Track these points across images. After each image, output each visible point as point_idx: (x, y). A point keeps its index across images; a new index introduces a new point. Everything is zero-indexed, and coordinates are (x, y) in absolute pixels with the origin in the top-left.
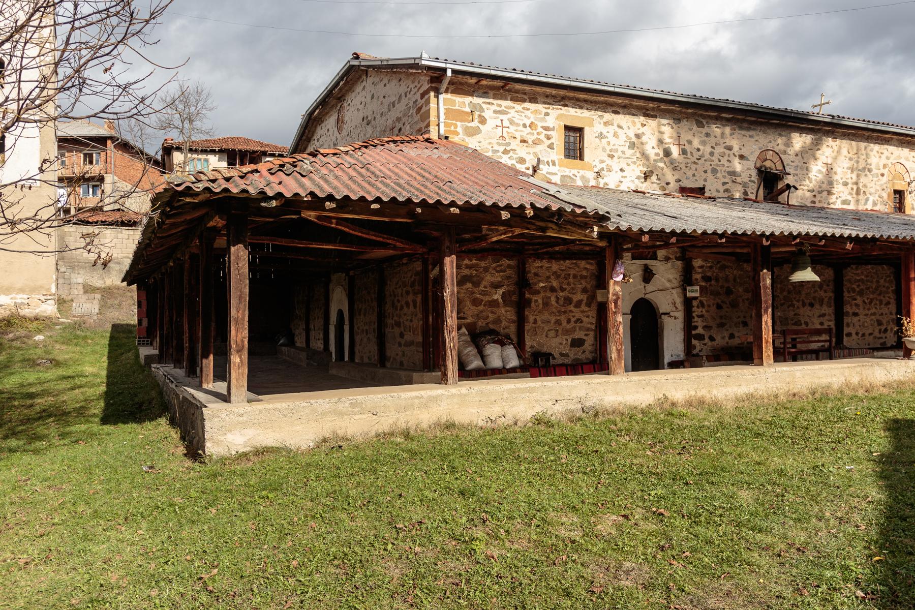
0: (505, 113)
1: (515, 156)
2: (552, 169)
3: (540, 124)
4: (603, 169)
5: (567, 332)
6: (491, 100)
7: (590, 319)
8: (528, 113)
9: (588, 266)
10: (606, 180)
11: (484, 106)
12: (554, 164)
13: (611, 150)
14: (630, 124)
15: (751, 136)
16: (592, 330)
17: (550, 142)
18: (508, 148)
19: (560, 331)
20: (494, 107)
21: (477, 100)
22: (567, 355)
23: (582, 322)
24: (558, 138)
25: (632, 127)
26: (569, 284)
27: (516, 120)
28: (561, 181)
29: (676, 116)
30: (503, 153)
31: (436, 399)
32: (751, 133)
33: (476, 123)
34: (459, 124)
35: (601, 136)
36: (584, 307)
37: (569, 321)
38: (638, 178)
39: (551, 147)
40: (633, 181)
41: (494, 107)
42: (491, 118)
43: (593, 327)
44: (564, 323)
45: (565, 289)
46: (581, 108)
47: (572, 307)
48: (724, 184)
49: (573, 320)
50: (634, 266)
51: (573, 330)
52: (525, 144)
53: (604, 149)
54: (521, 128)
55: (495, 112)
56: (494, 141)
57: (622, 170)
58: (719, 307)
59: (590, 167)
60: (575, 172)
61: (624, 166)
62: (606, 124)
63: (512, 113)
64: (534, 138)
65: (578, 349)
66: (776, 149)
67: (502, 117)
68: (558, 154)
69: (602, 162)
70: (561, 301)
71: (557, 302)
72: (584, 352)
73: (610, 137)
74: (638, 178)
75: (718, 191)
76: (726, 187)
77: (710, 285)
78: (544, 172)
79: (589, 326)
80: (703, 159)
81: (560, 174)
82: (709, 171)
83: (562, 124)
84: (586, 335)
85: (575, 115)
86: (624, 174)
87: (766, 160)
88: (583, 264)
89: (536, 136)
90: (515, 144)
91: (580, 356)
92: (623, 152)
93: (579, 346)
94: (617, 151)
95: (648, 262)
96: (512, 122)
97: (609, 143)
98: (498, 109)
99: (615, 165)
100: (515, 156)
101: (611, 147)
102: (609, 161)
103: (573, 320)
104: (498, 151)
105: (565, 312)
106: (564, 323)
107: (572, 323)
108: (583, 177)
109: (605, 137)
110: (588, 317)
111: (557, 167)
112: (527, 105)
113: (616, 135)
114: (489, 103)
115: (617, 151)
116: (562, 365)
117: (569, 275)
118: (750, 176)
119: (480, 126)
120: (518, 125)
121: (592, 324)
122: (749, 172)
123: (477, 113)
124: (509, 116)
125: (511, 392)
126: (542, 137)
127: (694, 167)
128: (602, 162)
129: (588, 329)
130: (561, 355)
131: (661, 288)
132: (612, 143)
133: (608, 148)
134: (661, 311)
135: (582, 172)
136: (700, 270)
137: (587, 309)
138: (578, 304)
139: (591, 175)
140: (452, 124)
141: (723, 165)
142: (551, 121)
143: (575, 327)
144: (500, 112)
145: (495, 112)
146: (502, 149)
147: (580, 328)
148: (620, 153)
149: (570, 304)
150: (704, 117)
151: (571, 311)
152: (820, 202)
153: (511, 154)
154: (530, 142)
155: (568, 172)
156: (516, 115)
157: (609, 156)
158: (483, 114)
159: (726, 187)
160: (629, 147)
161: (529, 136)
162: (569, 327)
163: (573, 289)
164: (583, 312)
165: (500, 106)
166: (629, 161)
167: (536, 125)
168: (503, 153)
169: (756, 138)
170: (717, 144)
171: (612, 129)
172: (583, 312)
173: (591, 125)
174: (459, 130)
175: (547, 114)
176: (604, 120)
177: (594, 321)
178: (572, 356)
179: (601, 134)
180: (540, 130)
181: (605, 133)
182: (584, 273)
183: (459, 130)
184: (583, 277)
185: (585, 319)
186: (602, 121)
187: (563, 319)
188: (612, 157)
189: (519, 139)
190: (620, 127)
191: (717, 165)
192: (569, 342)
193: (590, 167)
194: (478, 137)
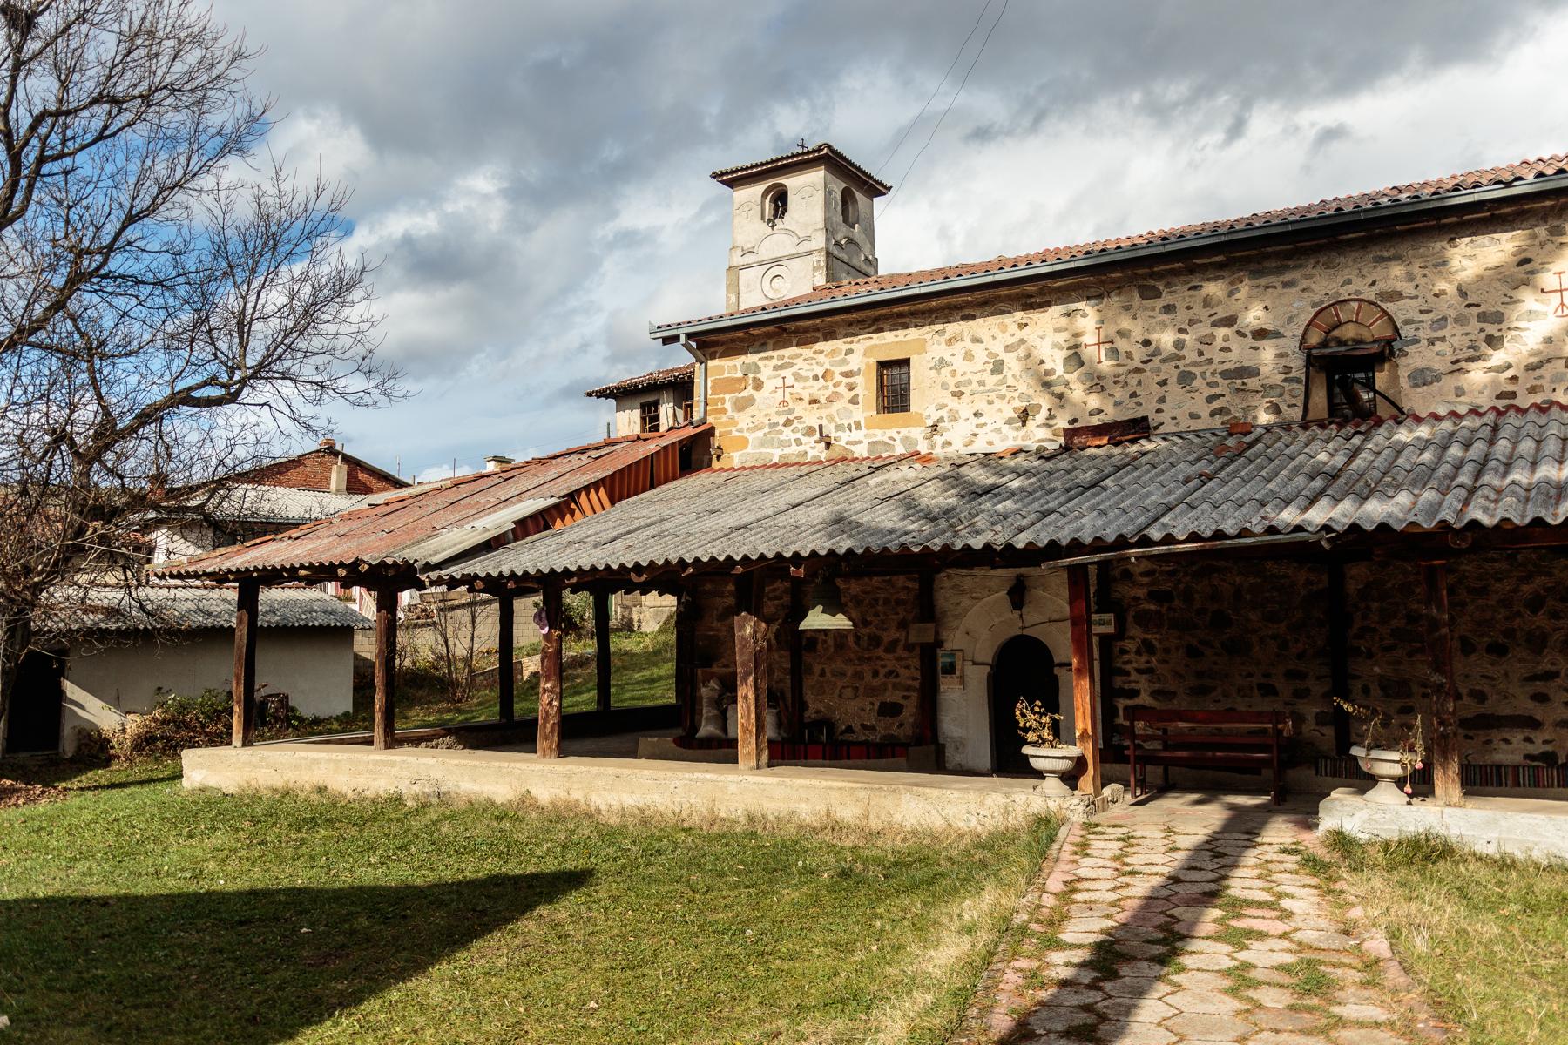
0: (790, 365)
1: (800, 426)
2: (856, 435)
3: (837, 370)
4: (941, 419)
5: (872, 691)
6: (770, 353)
7: (910, 673)
8: (821, 358)
9: (910, 584)
10: (946, 436)
11: (761, 364)
12: (858, 425)
13: (957, 385)
14: (995, 331)
15: (1285, 285)
16: (915, 690)
17: (853, 393)
18: (791, 417)
19: (861, 690)
20: (775, 362)
21: (752, 358)
22: (873, 728)
23: (897, 675)
24: (867, 386)
25: (1000, 336)
26: (876, 615)
27: (803, 373)
28: (869, 451)
29: (1093, 292)
30: (785, 425)
31: (317, 762)
32: (1287, 277)
33: (749, 391)
34: (727, 397)
35: (941, 364)
36: (900, 652)
37: (876, 674)
38: (1009, 422)
39: (854, 401)
40: (998, 430)
41: (775, 362)
42: (769, 378)
43: (917, 684)
44: (868, 677)
45: (870, 623)
46: (905, 326)
47: (880, 652)
48: (1210, 399)
49: (882, 672)
50: (997, 580)
51: (884, 687)
52: (816, 406)
53: (944, 386)
54: (811, 382)
55: (776, 368)
56: (773, 410)
57: (976, 414)
58: (1193, 653)
59: (919, 421)
60: (892, 433)
61: (981, 405)
62: (949, 342)
63: (799, 363)
64: (828, 393)
65: (891, 720)
66: (1370, 294)
67: (783, 373)
68: (866, 410)
69: (941, 407)
70: (864, 642)
71: (857, 643)
72: (901, 725)
73: (959, 364)
74: (1009, 422)
75: (1194, 416)
76: (1216, 405)
77: (1170, 609)
78: (843, 443)
79: (910, 682)
80: (1157, 360)
81: (866, 441)
82: (1173, 381)
83: (873, 361)
84: (905, 697)
85: (890, 342)
86: (981, 420)
87: (1339, 324)
88: (901, 581)
89: (832, 389)
90: (800, 409)
91: (895, 731)
92: (982, 383)
93: (893, 715)
94: (970, 382)
95: (1023, 570)
96: (798, 377)
97: (954, 373)
98: (780, 363)
99: (965, 408)
100: (800, 426)
101: (959, 378)
102: (953, 403)
103: (882, 672)
104: (777, 424)
105: (869, 659)
106: (868, 677)
107: (881, 678)
108: (905, 440)
109: (948, 365)
110: (907, 667)
111: (864, 431)
112: (820, 346)
113: (969, 356)
114: (767, 358)
115: (970, 382)
116: (866, 743)
117: (876, 600)
118: (1287, 369)
119: (755, 393)
120: (806, 379)
121: (914, 679)
122: (1284, 362)
123: (751, 376)
124: (794, 369)
125: (376, 763)
126: (842, 389)
127: (1133, 380)
128: (941, 407)
129: (908, 688)
130: (864, 726)
131: (1056, 616)
132: (960, 372)
133: (952, 382)
134: (1056, 660)
135: (904, 431)
136: (1145, 580)
137: (905, 654)
138: (892, 647)
139: (918, 433)
140: (719, 399)
141: (1210, 361)
142: (855, 362)
143: (885, 684)
144: (782, 367)
145: (776, 368)
146: (782, 420)
147: (895, 686)
148: (975, 386)
149: (878, 645)
150: (1153, 276)
151: (879, 658)
152: (1532, 390)
153: (796, 424)
154: (823, 400)
155: (880, 435)
156: (804, 365)
157: (954, 394)
158: (759, 376)
159: (1216, 405)
160: (993, 372)
161: (822, 392)
162: (875, 683)
163: (883, 622)
164: (899, 659)
165: (783, 357)
166: (992, 396)
167: (833, 373)
168: (785, 425)
169: (1305, 283)
170: (1192, 322)
171: (958, 348)
172: (899, 659)
173: (922, 347)
174: (728, 405)
175: (849, 352)
176: (947, 336)
177: (918, 674)
178: (881, 730)
179: (942, 360)
180: (838, 378)
181: (948, 358)
182: (903, 596)
183: (728, 405)
184: (899, 602)
185: (902, 671)
186: (943, 339)
187: (867, 669)
188: (958, 395)
189: (807, 399)
190: (976, 340)
191: (1194, 364)
192: (876, 707)
193: (919, 421)
194: (750, 411)
